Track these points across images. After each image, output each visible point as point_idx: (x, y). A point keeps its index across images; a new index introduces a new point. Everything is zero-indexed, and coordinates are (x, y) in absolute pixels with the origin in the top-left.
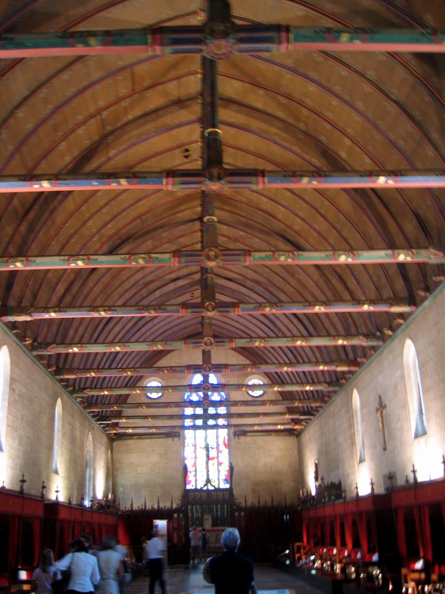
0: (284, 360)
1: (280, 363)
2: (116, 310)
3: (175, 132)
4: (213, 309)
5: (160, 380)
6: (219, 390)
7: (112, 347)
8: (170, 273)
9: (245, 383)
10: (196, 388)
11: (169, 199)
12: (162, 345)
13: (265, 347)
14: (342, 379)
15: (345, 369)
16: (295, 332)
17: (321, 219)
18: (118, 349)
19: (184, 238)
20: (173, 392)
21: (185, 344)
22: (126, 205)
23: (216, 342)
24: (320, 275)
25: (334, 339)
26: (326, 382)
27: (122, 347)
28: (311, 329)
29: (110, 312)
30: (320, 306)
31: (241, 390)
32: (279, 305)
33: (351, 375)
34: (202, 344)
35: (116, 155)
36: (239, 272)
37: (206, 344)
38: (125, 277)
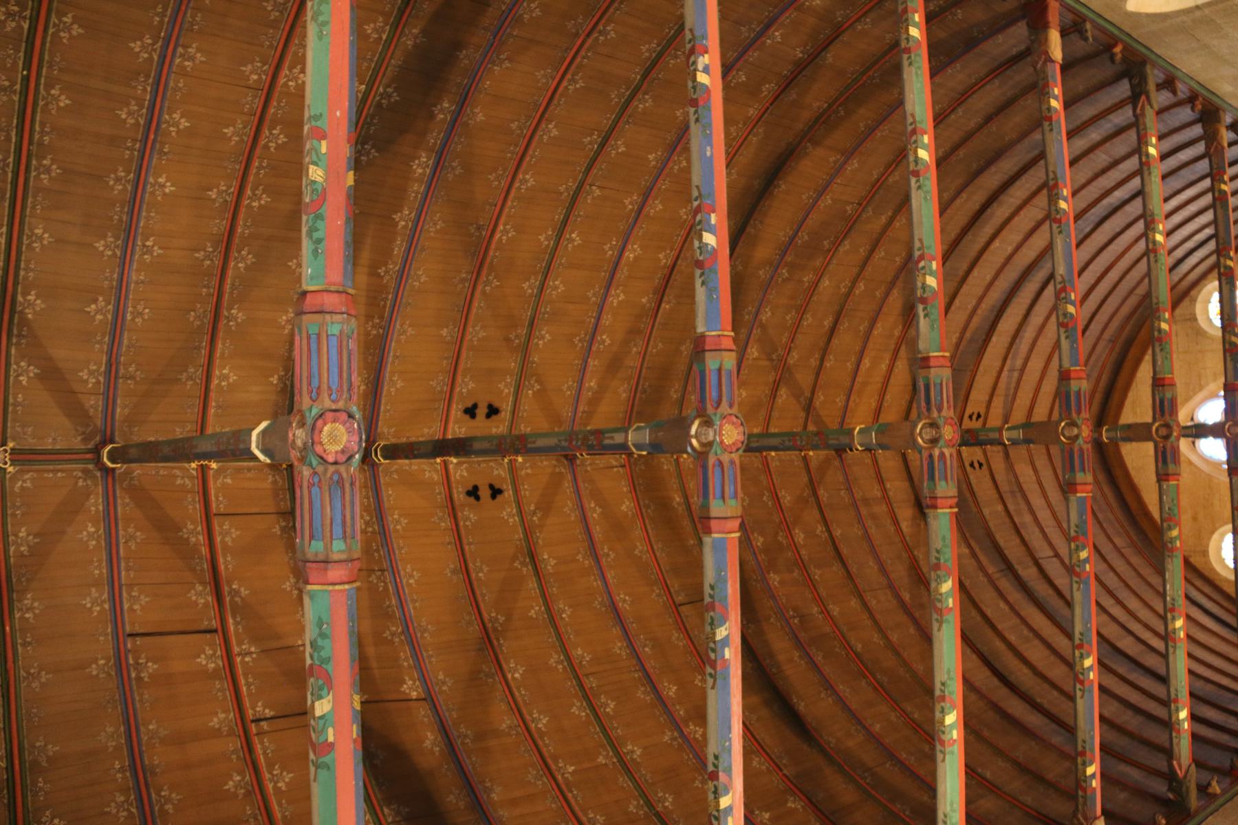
0: (1137, 240)
1: (1146, 253)
2: (716, 757)
3: (397, 522)
4: (708, 423)
5: (1216, 536)
6: (1168, 395)
7: (946, 737)
8: (896, 522)
9: (1220, 334)
10: (1165, 461)
11: (638, 532)
12: (940, 581)
13: (946, 258)
14: (1112, 58)
15: (1054, 37)
16: (1033, 213)
17: (619, 146)
18: (951, 718)
19: (782, 493)
20: (1178, 524)
21: (935, 507)
22: (619, 648)
23: (929, 410)
24: (816, 143)
25: (908, 50)
26: (1134, 99)
27: (947, 705)
28: (1007, 166)
29: (722, 777)
30: (696, 70)
31: (1169, 334)
32: (696, 204)
33: (1088, 26)
34: (936, 452)
35: (424, 679)
36: (887, 357)
37: (934, 441)
38: (876, 637)
